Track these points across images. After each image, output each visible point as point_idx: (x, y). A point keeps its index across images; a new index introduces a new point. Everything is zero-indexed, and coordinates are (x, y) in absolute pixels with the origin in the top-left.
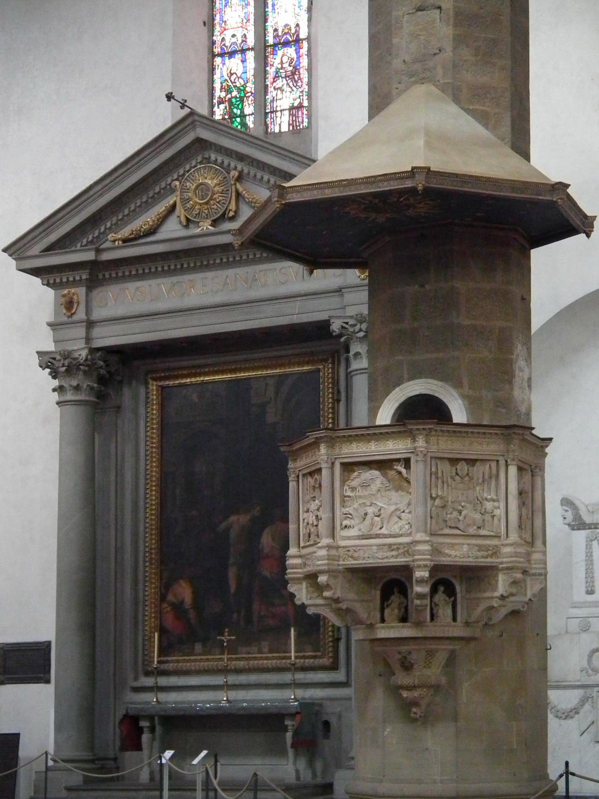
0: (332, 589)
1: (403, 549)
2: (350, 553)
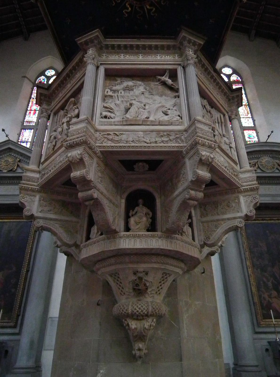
0: (85, 167)
1: (175, 136)
2: (110, 137)
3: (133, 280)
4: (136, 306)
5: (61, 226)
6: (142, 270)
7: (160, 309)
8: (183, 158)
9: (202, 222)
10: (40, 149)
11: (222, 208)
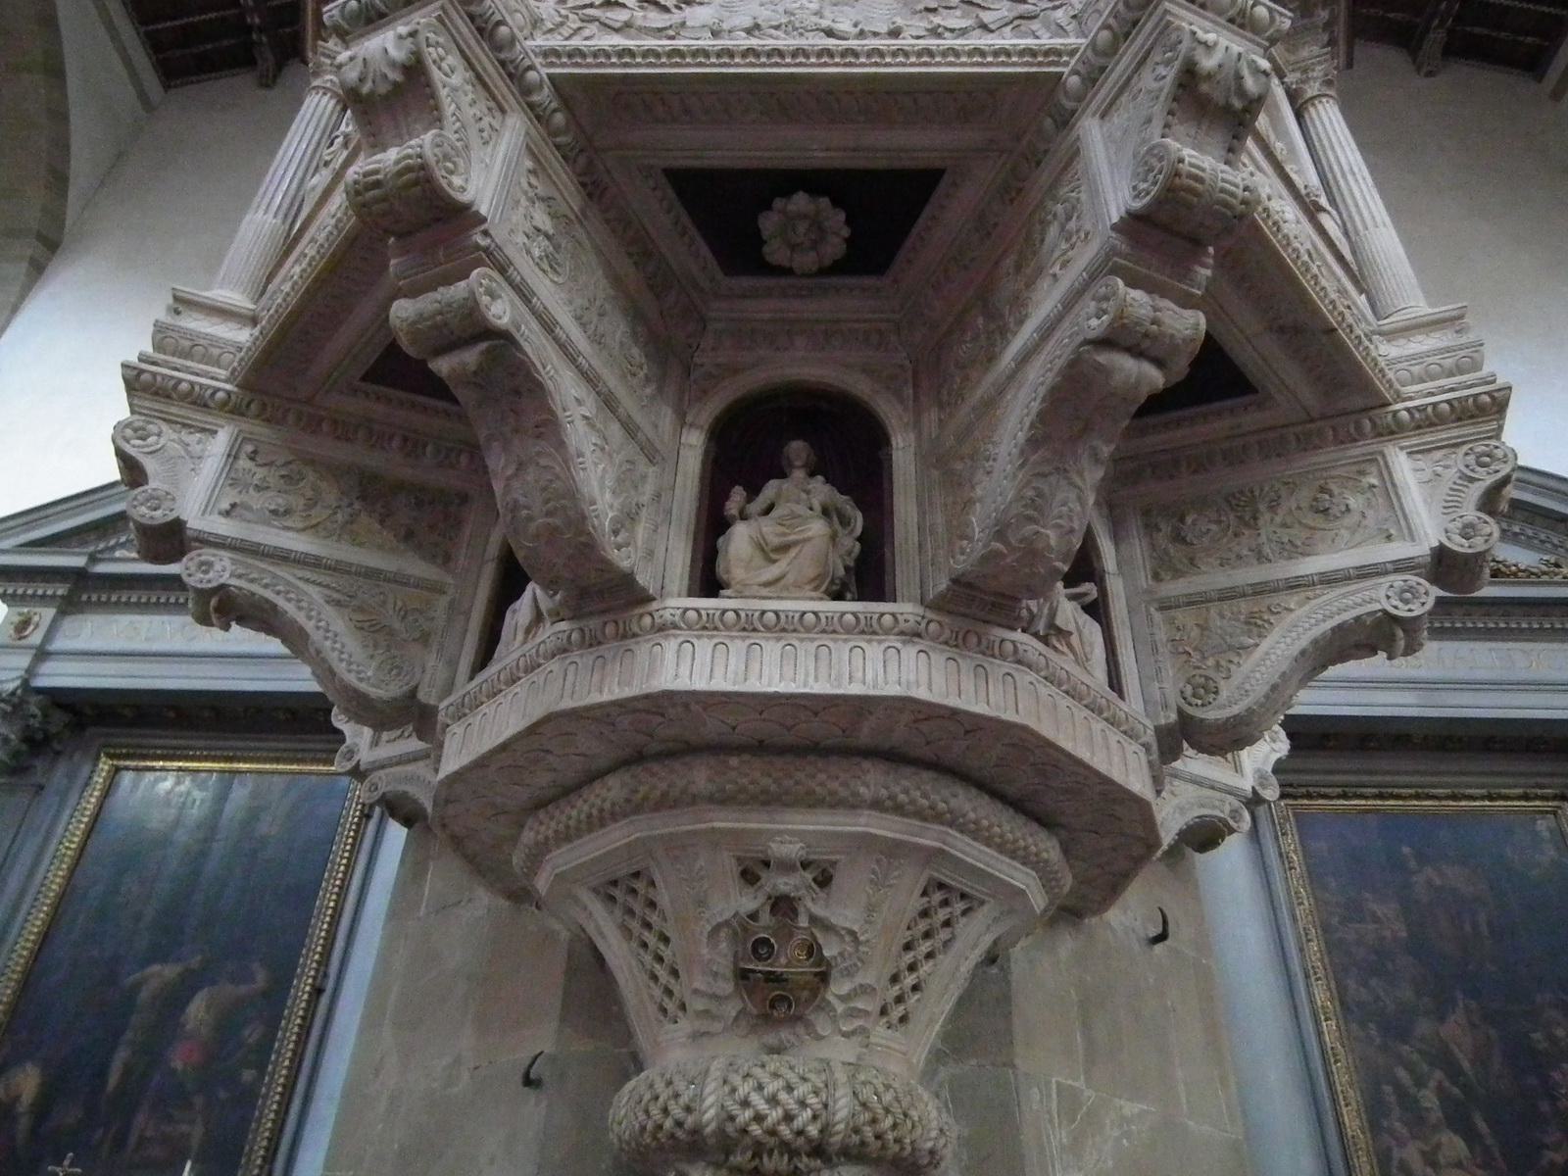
3: (736, 914)
4: (751, 1082)
5: (336, 596)
6: (793, 850)
7: (906, 1115)
8: (1065, 120)
9: (1165, 606)
10: (279, 221)
11: (1284, 525)
